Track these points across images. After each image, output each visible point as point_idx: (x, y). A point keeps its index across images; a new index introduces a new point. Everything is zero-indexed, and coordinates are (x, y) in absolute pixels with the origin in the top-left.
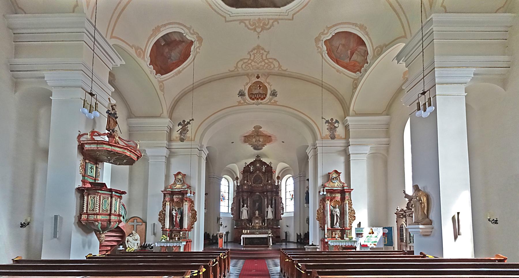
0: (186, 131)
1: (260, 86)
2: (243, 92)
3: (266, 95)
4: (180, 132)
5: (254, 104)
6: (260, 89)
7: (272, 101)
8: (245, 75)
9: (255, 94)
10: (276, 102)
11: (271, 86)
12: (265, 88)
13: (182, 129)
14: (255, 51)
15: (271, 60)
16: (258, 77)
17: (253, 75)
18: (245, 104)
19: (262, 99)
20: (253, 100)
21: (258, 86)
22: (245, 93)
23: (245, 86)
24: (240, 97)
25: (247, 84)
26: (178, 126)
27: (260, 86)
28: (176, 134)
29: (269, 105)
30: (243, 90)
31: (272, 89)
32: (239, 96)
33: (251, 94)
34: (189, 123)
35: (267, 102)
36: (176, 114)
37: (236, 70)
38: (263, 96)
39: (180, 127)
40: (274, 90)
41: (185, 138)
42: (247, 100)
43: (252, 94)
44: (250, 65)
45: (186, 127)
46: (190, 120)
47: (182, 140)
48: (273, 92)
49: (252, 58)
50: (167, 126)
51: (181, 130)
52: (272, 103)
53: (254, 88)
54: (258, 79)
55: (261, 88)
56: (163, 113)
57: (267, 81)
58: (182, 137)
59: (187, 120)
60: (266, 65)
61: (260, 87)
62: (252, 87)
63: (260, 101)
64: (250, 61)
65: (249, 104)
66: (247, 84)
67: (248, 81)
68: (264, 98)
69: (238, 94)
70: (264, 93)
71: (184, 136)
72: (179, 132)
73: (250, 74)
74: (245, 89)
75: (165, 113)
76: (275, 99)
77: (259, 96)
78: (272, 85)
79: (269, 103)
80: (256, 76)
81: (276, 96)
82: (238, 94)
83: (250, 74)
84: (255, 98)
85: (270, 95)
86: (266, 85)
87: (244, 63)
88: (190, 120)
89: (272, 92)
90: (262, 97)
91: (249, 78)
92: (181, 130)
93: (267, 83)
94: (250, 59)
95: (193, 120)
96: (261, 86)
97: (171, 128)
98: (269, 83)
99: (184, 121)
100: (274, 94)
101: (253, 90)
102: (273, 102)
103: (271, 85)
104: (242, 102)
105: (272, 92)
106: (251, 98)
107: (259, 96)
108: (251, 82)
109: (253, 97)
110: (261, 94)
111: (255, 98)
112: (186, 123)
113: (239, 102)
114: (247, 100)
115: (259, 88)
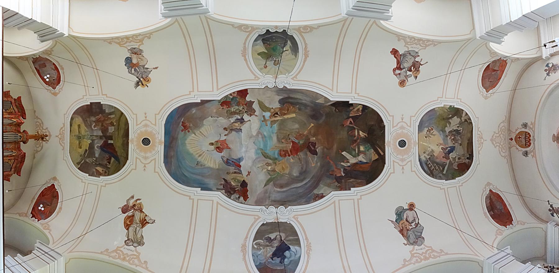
1: (518, 138)
3: (526, 132)
5: (534, 143)
6: (521, 138)
7: (531, 126)
8: (510, 150)
9: (525, 142)
10: (532, 124)
11: (518, 128)
13: (557, 213)
14: (494, 142)
15: (500, 130)
16: (511, 139)
17: (509, 143)
18: (534, 151)
19: (530, 136)
20: (530, 144)
21: (518, 139)
23: (519, 151)
24: (529, 155)
25: (517, 149)
26: (554, 216)
27: (518, 138)
29: (534, 130)
30: (522, 152)
31: (521, 127)
32: (528, 156)
33: (526, 146)
34: (551, 206)
35: (532, 132)
36: (544, 218)
37: (506, 157)
38: (527, 135)
39: (555, 214)
40: (522, 125)
42: (531, 149)
43: (525, 144)
44: (503, 146)
45: (555, 209)
46: (549, 204)
48: (524, 127)
49: (498, 145)
50: (554, 227)
52: (533, 127)
54: (513, 139)
55: (520, 136)
56: (542, 228)
57: (514, 131)
60: (503, 133)
61: (519, 138)
62: (520, 145)
63: (531, 138)
64: (501, 146)
65: (534, 148)
68: (529, 134)
70: (524, 134)
73: (510, 146)
74: (521, 151)
75: (543, 226)
76: (529, 124)
77: (527, 139)
78: (518, 128)
79: (533, 129)
80: (510, 141)
81: (527, 123)
82: (526, 156)
83: (510, 146)
84: (529, 142)
86: (517, 132)
87: (502, 151)
88: (549, 204)
89: (523, 127)
90: (528, 136)
92: (558, 215)
94: (499, 146)
95: (548, 201)
97: (556, 224)
98: (516, 130)
100: (525, 125)
101: (522, 143)
102: (532, 126)
103: (518, 128)
104: (532, 154)
105: (523, 127)
106: (529, 146)
107: (527, 139)
108: (515, 145)
109: (528, 144)
110: (525, 137)
111: (529, 142)
112: (551, 209)
113: (533, 156)
114: (531, 149)
115: (520, 139)
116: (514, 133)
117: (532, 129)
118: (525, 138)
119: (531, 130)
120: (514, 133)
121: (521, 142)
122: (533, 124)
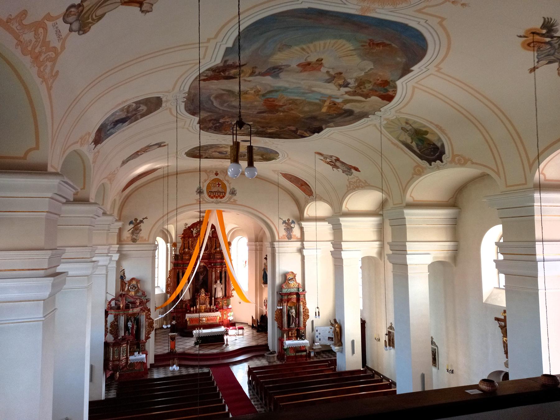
0: (138, 231)
1: (219, 183)
2: (202, 190)
3: (225, 193)
4: (132, 232)
5: (213, 202)
6: (219, 186)
7: (232, 200)
9: (214, 192)
10: (235, 201)
12: (224, 187)
13: (135, 228)
17: (211, 171)
18: (204, 202)
19: (221, 198)
20: (212, 198)
21: (217, 183)
22: (203, 191)
27: (219, 183)
28: (127, 234)
29: (228, 203)
31: (231, 188)
33: (209, 192)
34: (141, 222)
38: (222, 194)
39: (132, 226)
41: (137, 239)
42: (206, 198)
43: (211, 192)
46: (144, 219)
47: (134, 241)
51: (132, 229)
52: (232, 202)
53: (213, 185)
54: (217, 175)
55: (220, 186)
58: (134, 237)
59: (140, 219)
61: (219, 185)
62: (210, 185)
63: (219, 199)
66: (206, 181)
67: (207, 178)
68: (224, 197)
69: (197, 192)
70: (223, 191)
71: (136, 236)
72: (131, 231)
73: (208, 171)
76: (235, 198)
79: (229, 202)
80: (215, 172)
81: (235, 195)
82: (197, 192)
83: (208, 171)
85: (230, 194)
88: (144, 219)
89: (231, 190)
90: (221, 195)
91: (207, 175)
92: (132, 229)
93: (226, 180)
95: (146, 218)
96: (220, 183)
99: (136, 220)
100: (233, 193)
101: (212, 188)
102: (233, 201)
106: (210, 196)
108: (209, 179)
109: (212, 195)
110: (219, 192)
112: (138, 221)
115: (218, 186)
116: (225, 178)
117: (229, 200)
118: (219, 192)
119: (228, 199)
120: (225, 178)
121: (214, 187)
122: (234, 203)
